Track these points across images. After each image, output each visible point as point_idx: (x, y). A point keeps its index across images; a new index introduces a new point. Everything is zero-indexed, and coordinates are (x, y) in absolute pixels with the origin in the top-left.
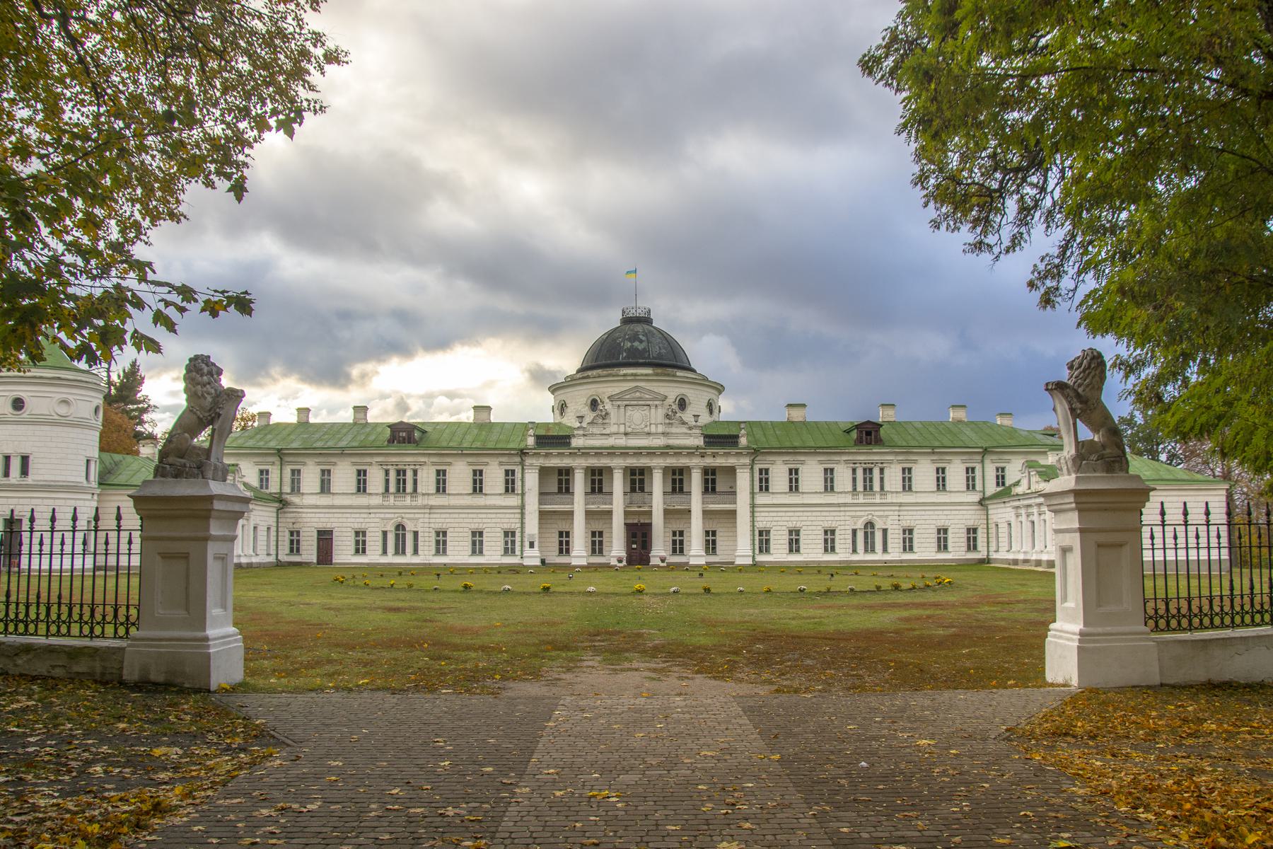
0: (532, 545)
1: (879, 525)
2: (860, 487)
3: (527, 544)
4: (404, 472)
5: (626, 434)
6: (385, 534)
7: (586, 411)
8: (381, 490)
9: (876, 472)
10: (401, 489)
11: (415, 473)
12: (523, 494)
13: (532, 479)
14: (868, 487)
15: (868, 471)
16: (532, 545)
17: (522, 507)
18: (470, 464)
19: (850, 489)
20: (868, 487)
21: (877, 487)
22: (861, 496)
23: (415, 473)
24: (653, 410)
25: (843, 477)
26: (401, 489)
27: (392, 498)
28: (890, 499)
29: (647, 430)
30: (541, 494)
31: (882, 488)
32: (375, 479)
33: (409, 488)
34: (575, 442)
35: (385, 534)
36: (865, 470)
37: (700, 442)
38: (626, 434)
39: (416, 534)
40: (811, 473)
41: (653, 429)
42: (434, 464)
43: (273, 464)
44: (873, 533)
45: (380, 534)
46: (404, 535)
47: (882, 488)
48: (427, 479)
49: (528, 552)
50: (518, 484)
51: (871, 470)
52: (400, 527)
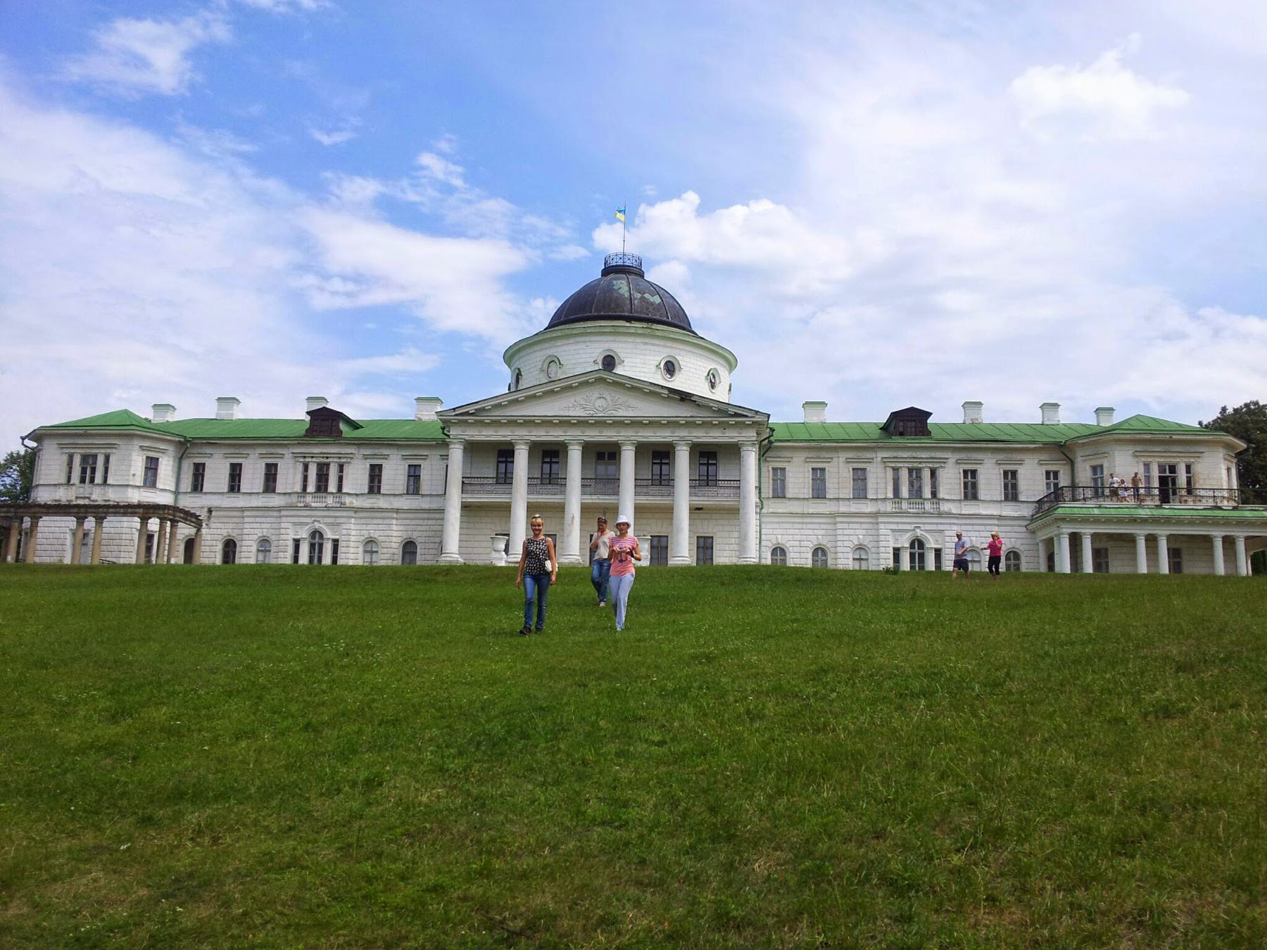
1: (931, 543)
2: (905, 492)
4: (328, 465)
6: (297, 543)
8: (298, 488)
9: (926, 474)
10: (322, 486)
11: (341, 467)
14: (916, 493)
15: (915, 473)
18: (405, 458)
19: (890, 495)
20: (916, 493)
21: (927, 493)
22: (905, 505)
23: (341, 467)
25: (879, 480)
26: (322, 486)
27: (309, 499)
28: (945, 507)
31: (934, 494)
32: (289, 477)
33: (332, 487)
35: (297, 543)
36: (910, 470)
39: (336, 543)
40: (839, 474)
42: (365, 457)
43: (163, 452)
44: (922, 556)
45: (291, 545)
46: (321, 546)
47: (934, 494)
48: (356, 477)
51: (919, 470)
52: (316, 535)
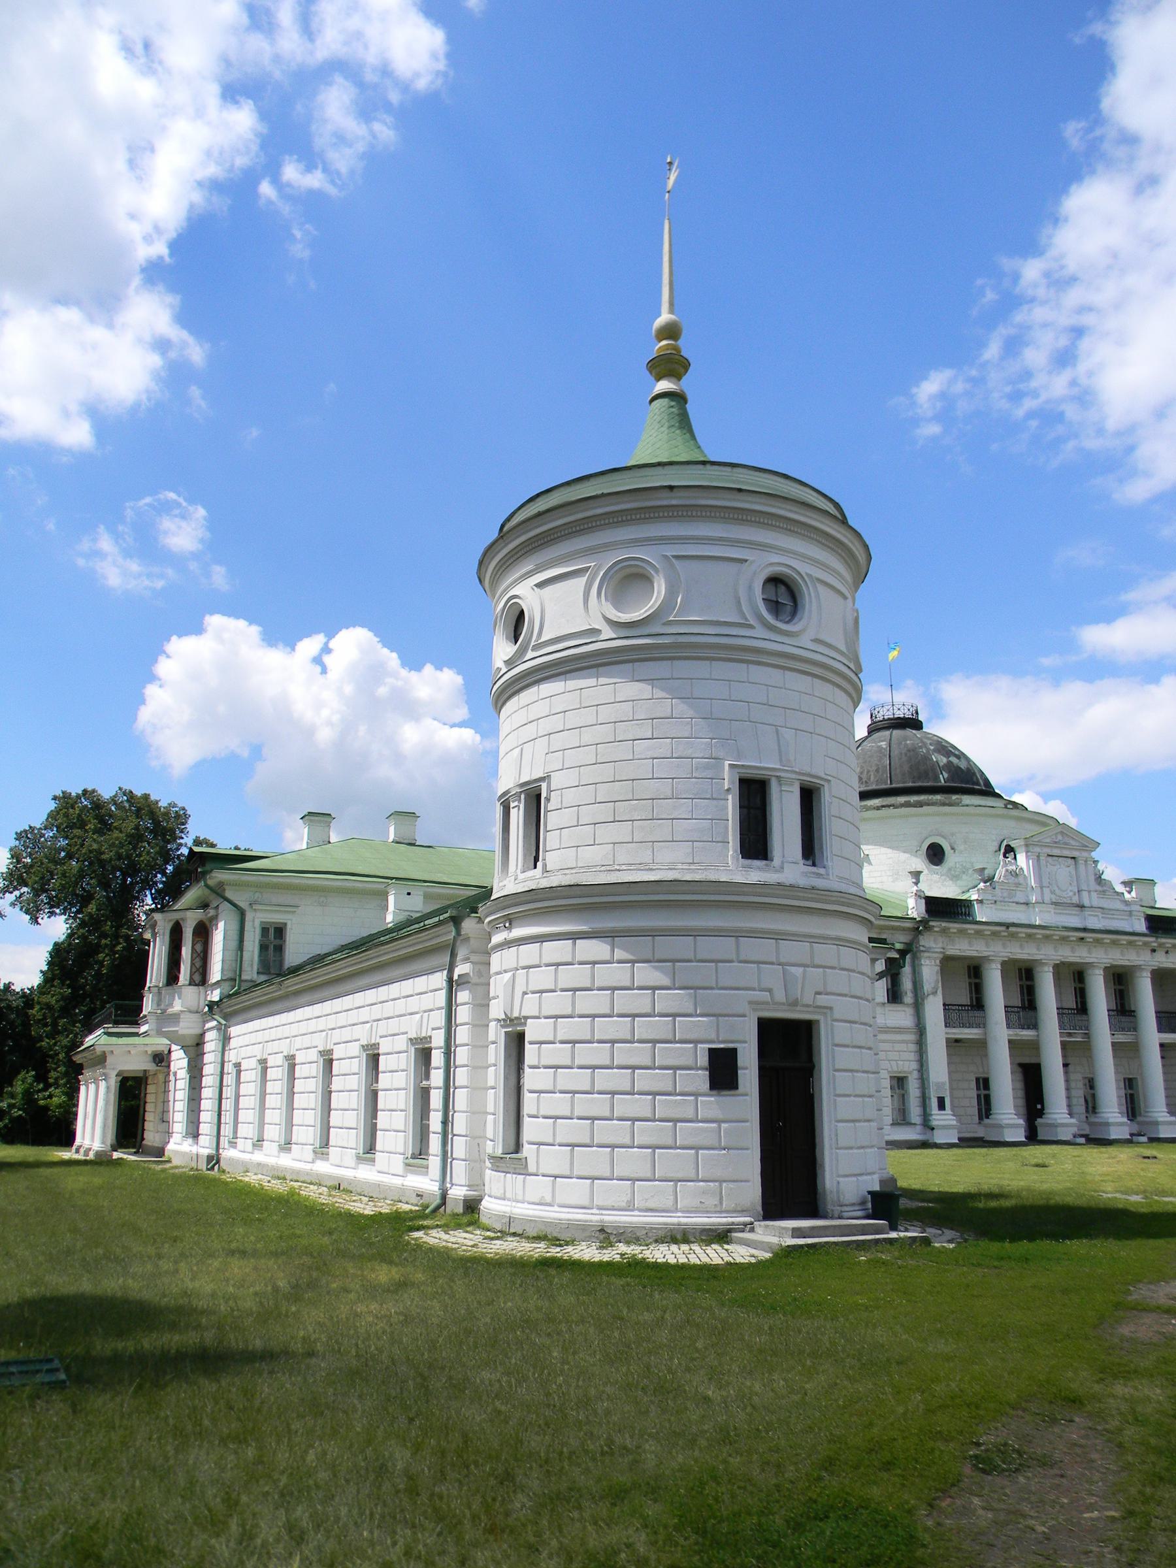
0: (941, 1105)
3: (934, 1103)
5: (1055, 904)
7: (919, 863)
12: (918, 1007)
13: (930, 972)
16: (941, 1105)
17: (920, 1030)
24: (1082, 868)
29: (1075, 900)
30: (944, 1005)
34: (981, 914)
37: (1141, 926)
38: (1055, 904)
41: (1086, 903)
49: (939, 1118)
50: (907, 984)
